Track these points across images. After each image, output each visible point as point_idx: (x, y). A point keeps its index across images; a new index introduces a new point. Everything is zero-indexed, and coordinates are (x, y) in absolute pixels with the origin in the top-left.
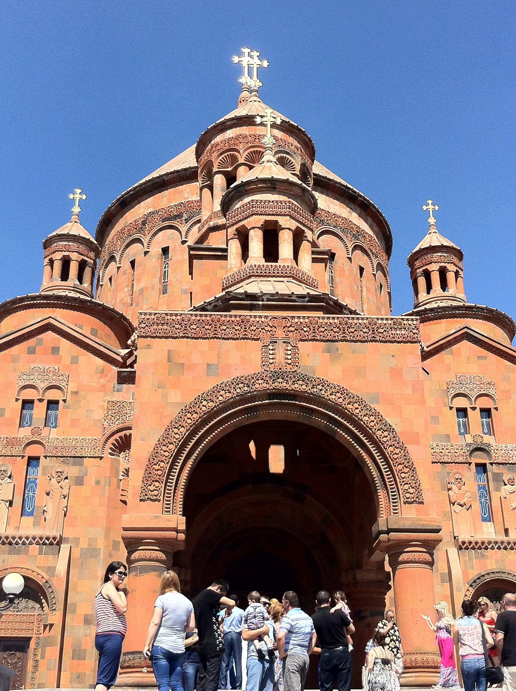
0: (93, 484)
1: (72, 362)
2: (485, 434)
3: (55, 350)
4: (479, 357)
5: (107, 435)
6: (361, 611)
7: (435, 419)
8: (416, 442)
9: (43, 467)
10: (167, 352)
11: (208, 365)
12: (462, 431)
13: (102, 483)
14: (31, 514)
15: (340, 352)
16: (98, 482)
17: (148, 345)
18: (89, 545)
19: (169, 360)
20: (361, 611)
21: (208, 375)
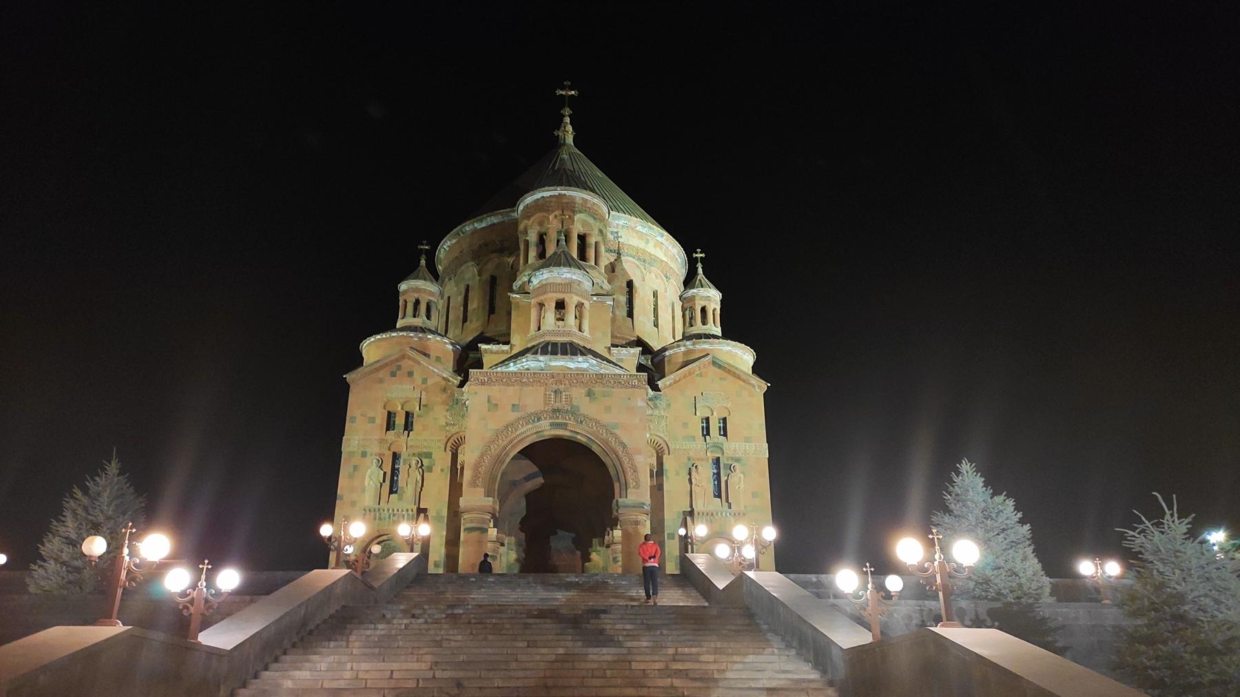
0: (439, 471)
1: (423, 383)
2: (720, 435)
3: (410, 374)
4: (721, 379)
5: (448, 437)
6: (616, 558)
7: (685, 425)
8: (639, 453)
9: (404, 459)
10: (487, 397)
11: (513, 405)
12: (705, 433)
13: (446, 471)
14: (396, 492)
15: (596, 396)
16: (442, 470)
17: (476, 393)
18: (437, 513)
19: (489, 401)
20: (616, 558)
21: (513, 411)
